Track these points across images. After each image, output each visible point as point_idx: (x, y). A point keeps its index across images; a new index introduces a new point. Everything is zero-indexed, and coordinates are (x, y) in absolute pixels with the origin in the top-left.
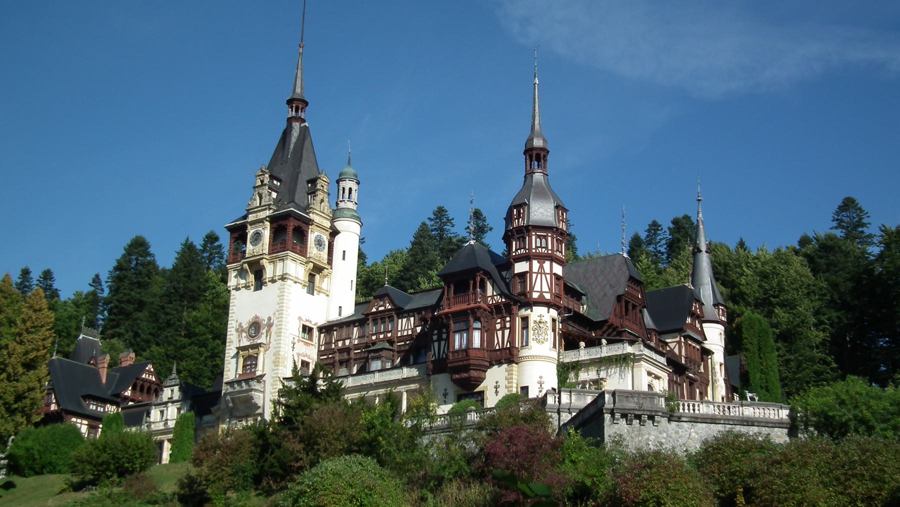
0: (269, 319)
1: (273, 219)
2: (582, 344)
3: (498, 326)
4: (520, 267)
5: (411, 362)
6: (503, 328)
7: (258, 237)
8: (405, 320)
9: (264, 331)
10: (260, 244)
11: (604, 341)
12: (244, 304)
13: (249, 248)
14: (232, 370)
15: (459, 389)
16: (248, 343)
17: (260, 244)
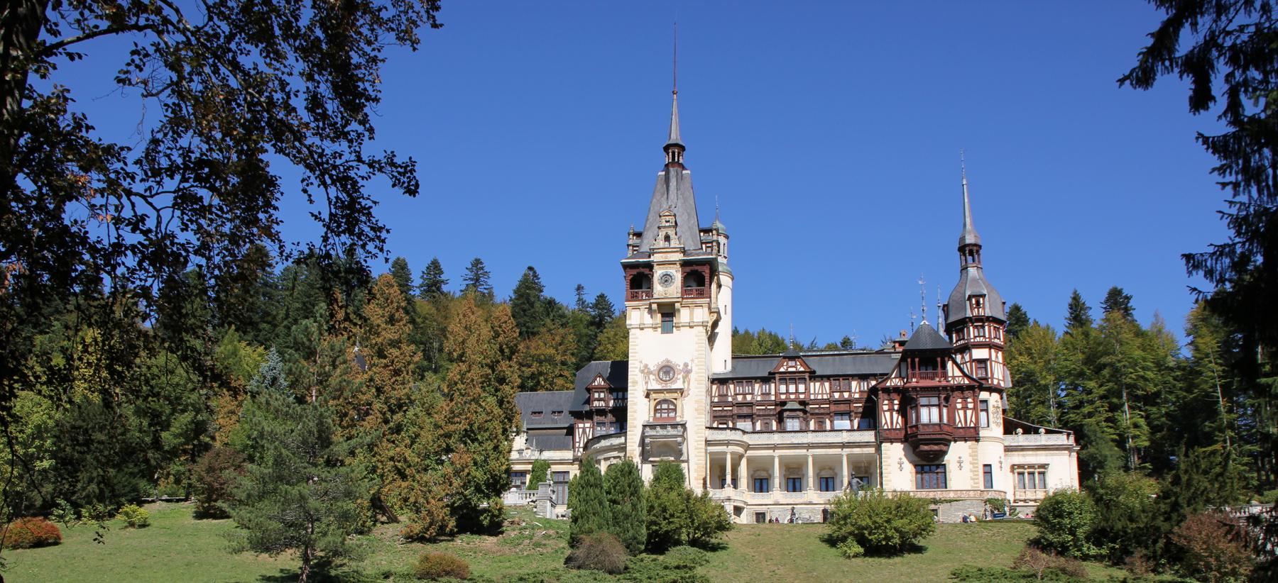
0: (686, 365)
1: (684, 264)
2: (1020, 430)
3: (959, 406)
4: (979, 354)
5: (828, 427)
6: (965, 408)
7: (667, 279)
8: (818, 384)
9: (680, 376)
10: (668, 285)
11: (1042, 430)
12: (647, 346)
13: (658, 289)
14: (639, 411)
15: (916, 459)
16: (659, 387)
17: (668, 285)
